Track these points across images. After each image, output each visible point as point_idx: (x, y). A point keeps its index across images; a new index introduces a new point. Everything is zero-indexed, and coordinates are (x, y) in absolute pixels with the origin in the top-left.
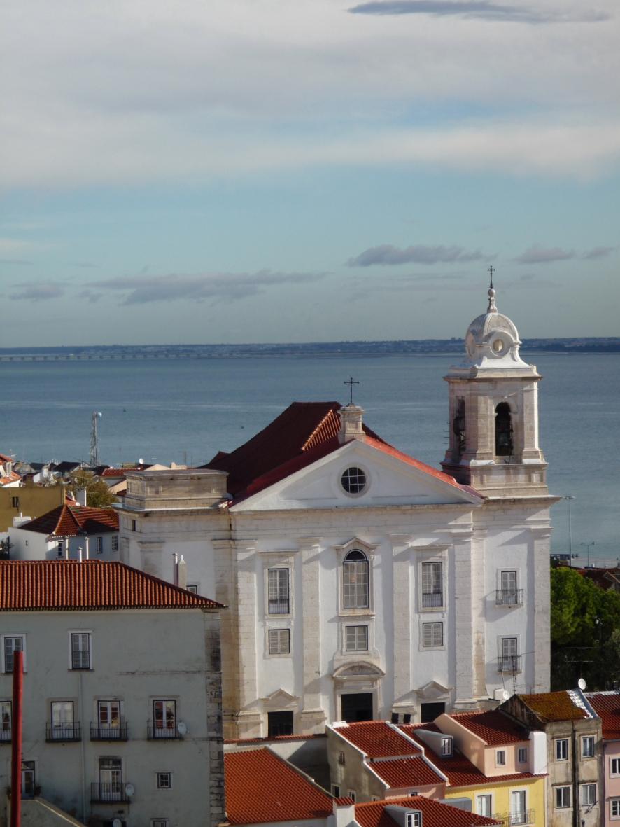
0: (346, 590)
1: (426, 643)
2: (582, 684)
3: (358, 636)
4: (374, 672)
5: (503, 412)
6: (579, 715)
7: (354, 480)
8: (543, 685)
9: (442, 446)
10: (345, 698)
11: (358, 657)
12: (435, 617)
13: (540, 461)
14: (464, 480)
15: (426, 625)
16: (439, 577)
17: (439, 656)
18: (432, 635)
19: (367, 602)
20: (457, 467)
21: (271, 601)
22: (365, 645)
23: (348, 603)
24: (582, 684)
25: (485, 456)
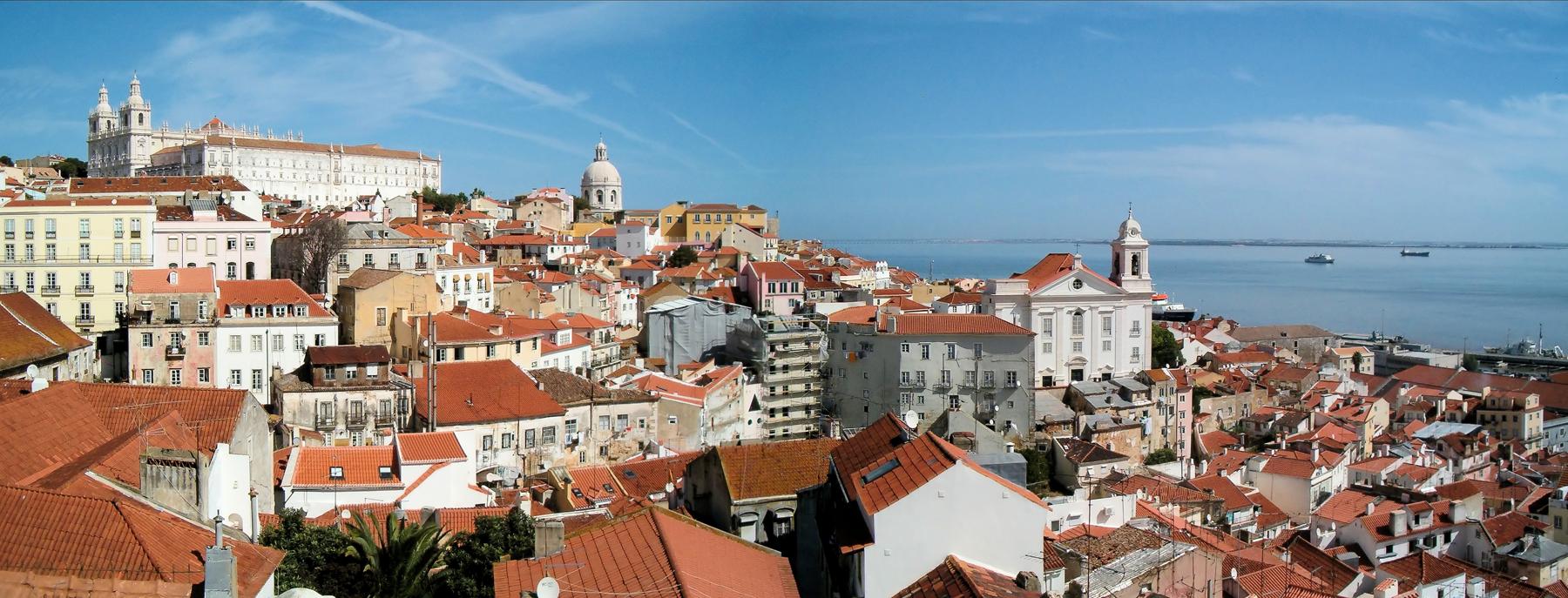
0: (1074, 328)
1: (1104, 349)
2: (1168, 366)
3: (1078, 346)
4: (1083, 361)
5: (1135, 259)
6: (1167, 379)
7: (1078, 284)
8: (1148, 368)
9: (1110, 269)
10: (1073, 371)
11: (1078, 355)
12: (1108, 339)
13: (1149, 278)
14: (1120, 285)
15: (1104, 342)
16: (1110, 323)
17: (1111, 354)
18: (1107, 346)
19: (1081, 332)
20: (1116, 277)
21: (1045, 332)
22: (1080, 350)
23: (1074, 332)
24: (1168, 366)
25: (1127, 275)
